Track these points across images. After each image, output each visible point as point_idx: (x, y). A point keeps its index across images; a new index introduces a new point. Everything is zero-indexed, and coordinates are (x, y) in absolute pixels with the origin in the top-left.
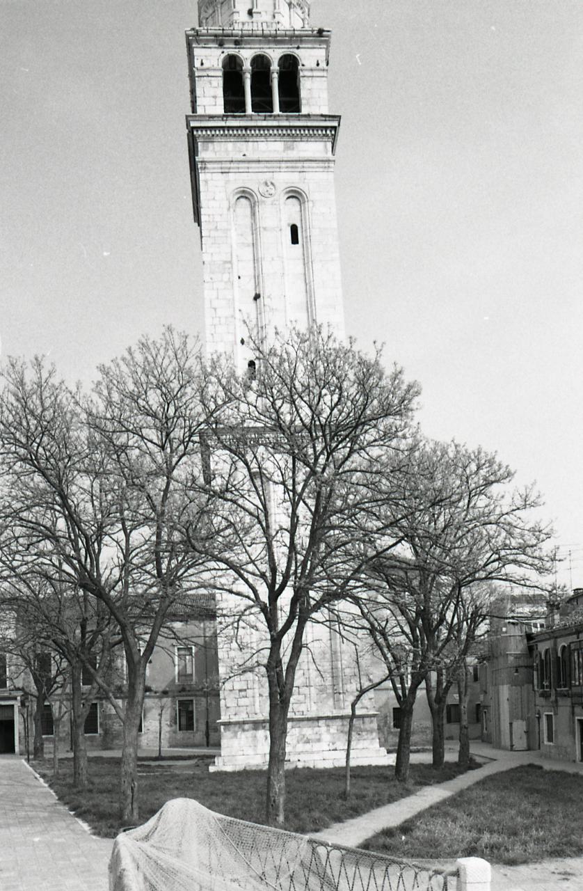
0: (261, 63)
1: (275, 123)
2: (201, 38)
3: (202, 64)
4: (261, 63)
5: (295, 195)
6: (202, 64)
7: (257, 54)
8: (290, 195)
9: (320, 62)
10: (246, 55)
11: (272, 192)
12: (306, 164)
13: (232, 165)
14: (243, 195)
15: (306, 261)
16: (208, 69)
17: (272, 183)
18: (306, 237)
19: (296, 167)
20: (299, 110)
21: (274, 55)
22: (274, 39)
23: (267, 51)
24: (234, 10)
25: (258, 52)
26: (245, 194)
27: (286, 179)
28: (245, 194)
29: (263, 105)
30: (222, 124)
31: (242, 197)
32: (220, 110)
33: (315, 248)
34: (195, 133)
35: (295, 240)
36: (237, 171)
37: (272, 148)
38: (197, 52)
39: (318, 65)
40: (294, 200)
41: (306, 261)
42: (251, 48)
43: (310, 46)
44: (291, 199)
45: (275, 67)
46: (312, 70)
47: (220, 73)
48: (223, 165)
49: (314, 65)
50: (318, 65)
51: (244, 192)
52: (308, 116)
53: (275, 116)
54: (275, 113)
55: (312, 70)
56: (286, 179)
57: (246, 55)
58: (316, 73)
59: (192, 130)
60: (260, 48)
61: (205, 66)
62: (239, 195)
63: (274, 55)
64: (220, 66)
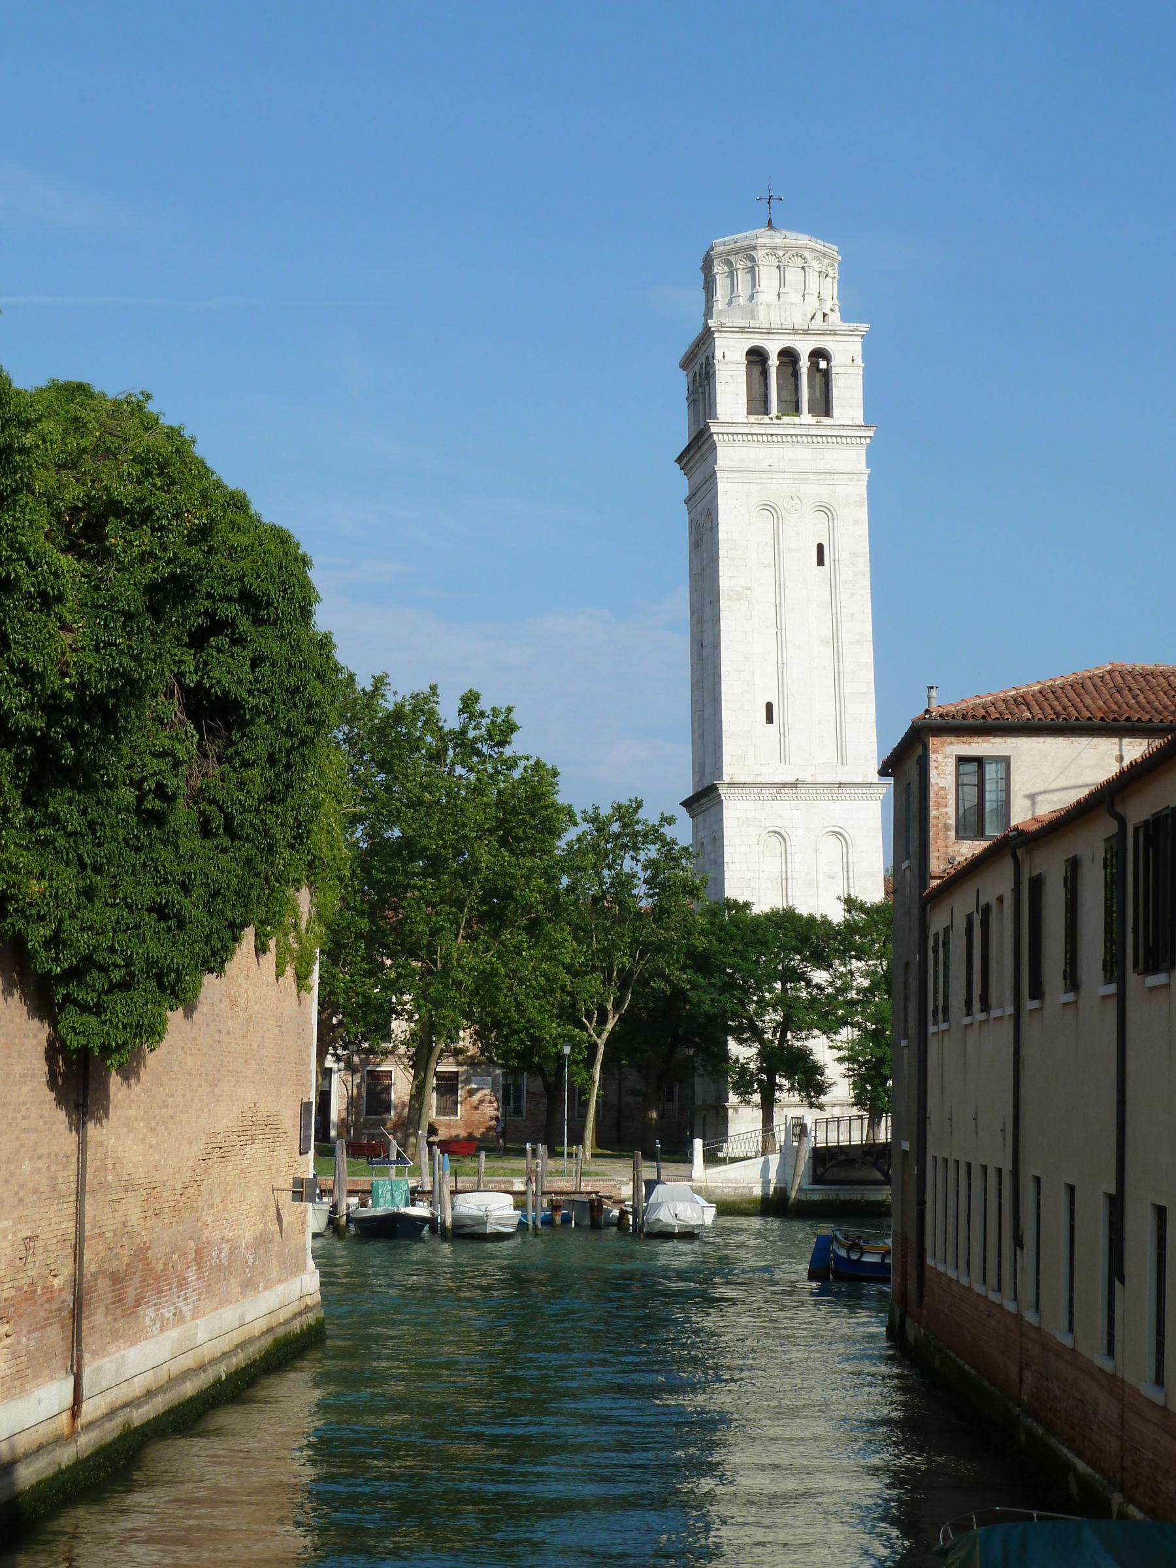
0: (789, 356)
5: (826, 510)
10: (773, 348)
12: (836, 477)
13: (755, 475)
15: (833, 584)
18: (834, 561)
19: (825, 480)
21: (804, 348)
27: (813, 490)
28: (769, 507)
33: (845, 573)
37: (801, 456)
41: (833, 584)
45: (804, 363)
57: (773, 348)
63: (804, 348)
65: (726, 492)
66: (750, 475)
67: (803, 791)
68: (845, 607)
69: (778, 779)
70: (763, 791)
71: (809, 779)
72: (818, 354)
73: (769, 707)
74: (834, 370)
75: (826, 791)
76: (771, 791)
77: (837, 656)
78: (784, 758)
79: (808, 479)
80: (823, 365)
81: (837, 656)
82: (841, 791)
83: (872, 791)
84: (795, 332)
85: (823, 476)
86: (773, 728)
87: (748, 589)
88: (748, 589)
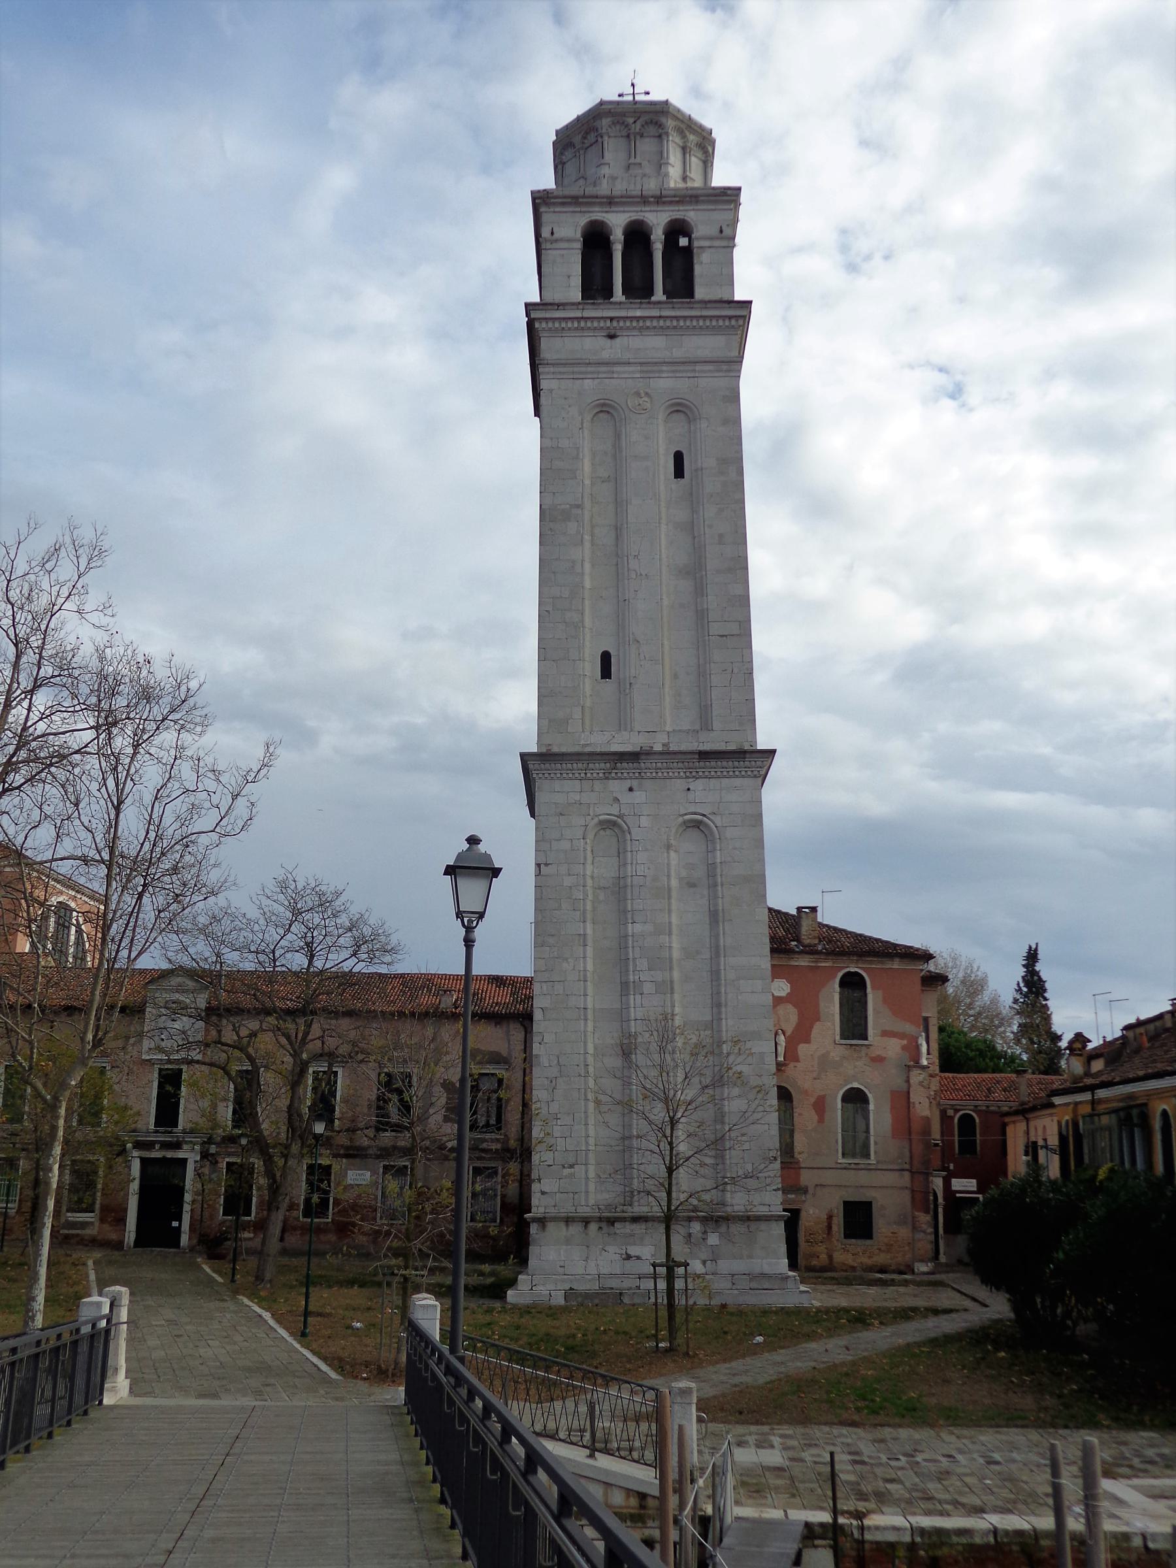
0: (637, 235)
1: (655, 313)
2: (552, 200)
3: (552, 233)
4: (637, 235)
5: (680, 409)
6: (552, 233)
7: (633, 218)
8: (676, 409)
9: (724, 228)
10: (617, 222)
11: (648, 405)
12: (698, 368)
13: (590, 369)
14: (604, 409)
16: (561, 240)
17: (647, 394)
20: (690, 293)
21: (658, 221)
22: (659, 200)
23: (647, 215)
24: (603, 161)
25: (635, 217)
26: (605, 409)
28: (605, 409)
29: (639, 289)
30: (578, 314)
31: (601, 411)
32: (577, 296)
34: (537, 325)
35: (679, 472)
36: (596, 376)
37: (653, 345)
38: (545, 218)
39: (721, 231)
40: (682, 416)
42: (624, 212)
43: (713, 207)
44: (675, 416)
46: (711, 238)
47: (579, 245)
48: (576, 369)
49: (714, 231)
50: (721, 231)
51: (604, 405)
52: (706, 303)
53: (616, 303)
54: (653, 299)
55: (711, 238)
56: (664, 384)
57: (617, 222)
58: (717, 243)
59: (530, 325)
60: (637, 212)
61: (556, 235)
62: (598, 410)
63: (658, 221)
64: (579, 235)
65: (551, 391)
66: (583, 369)
67: (649, 765)
68: (710, 526)
69: (615, 748)
70: (591, 766)
71: (658, 748)
72: (677, 229)
73: (606, 658)
74: (696, 244)
75: (680, 765)
76: (602, 765)
77: (700, 590)
78: (623, 724)
79: (661, 371)
80: (683, 242)
81: (700, 590)
82: (702, 764)
83: (747, 763)
84: (644, 200)
85: (681, 368)
86: (609, 686)
87: (578, 506)
88: (578, 506)
